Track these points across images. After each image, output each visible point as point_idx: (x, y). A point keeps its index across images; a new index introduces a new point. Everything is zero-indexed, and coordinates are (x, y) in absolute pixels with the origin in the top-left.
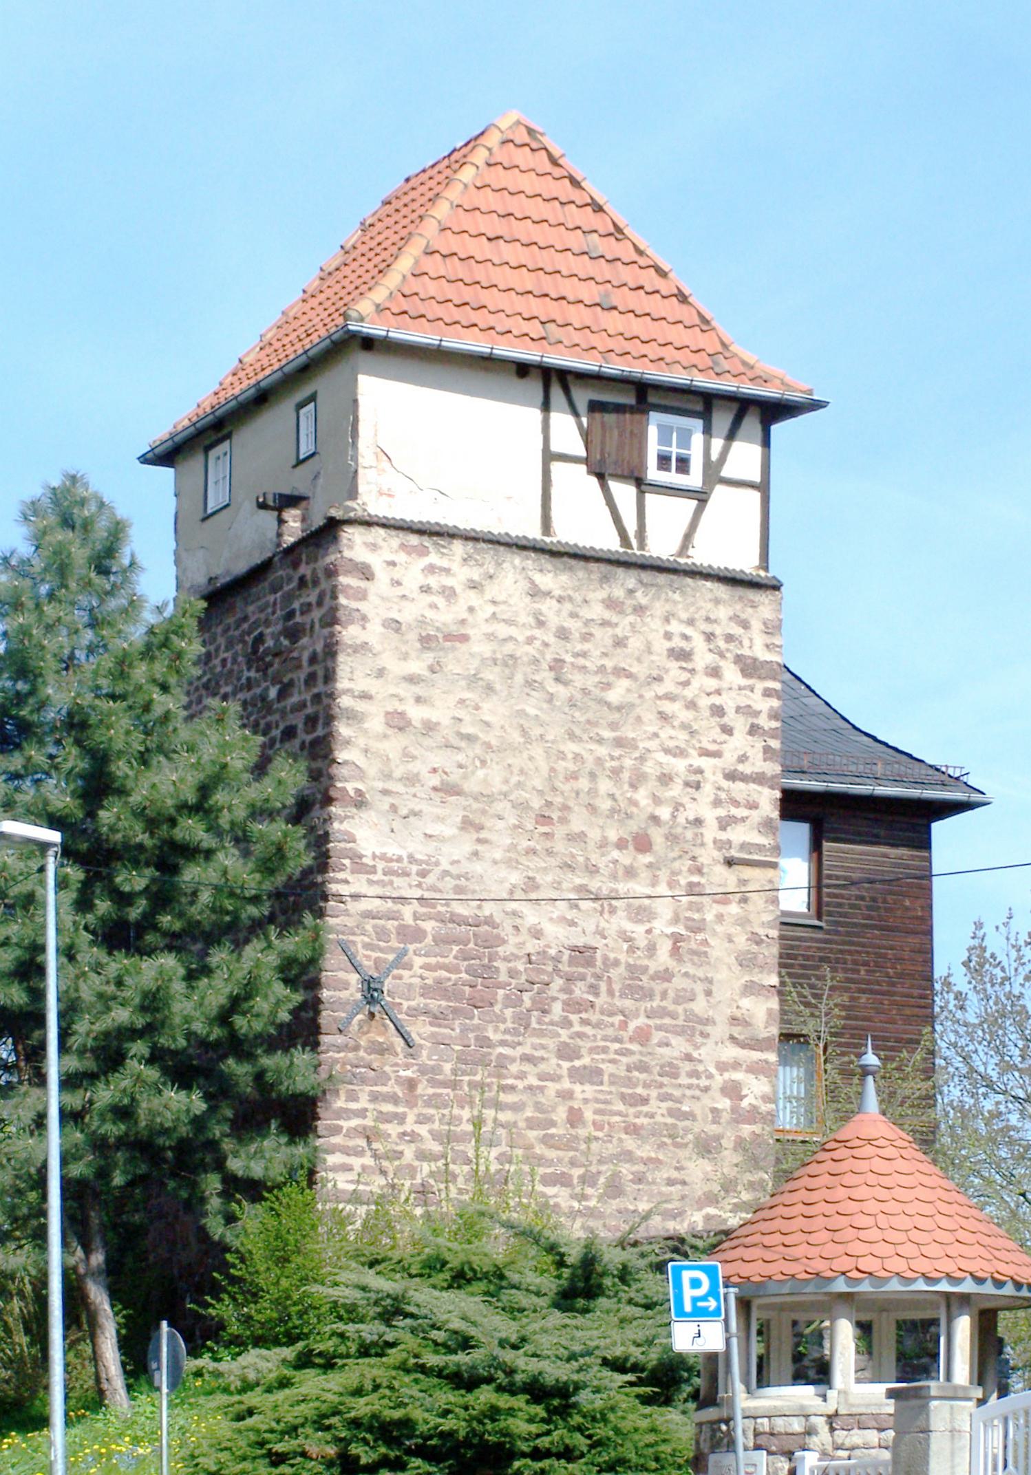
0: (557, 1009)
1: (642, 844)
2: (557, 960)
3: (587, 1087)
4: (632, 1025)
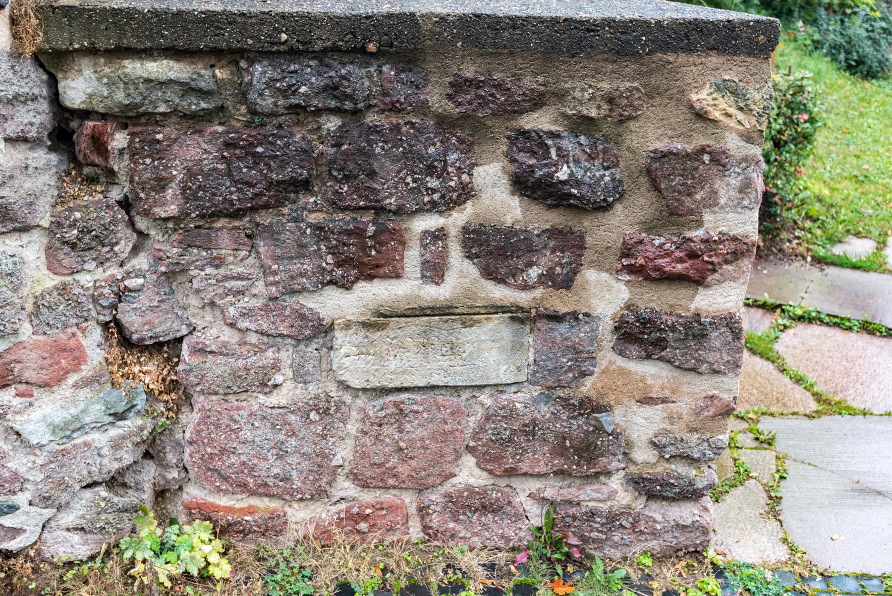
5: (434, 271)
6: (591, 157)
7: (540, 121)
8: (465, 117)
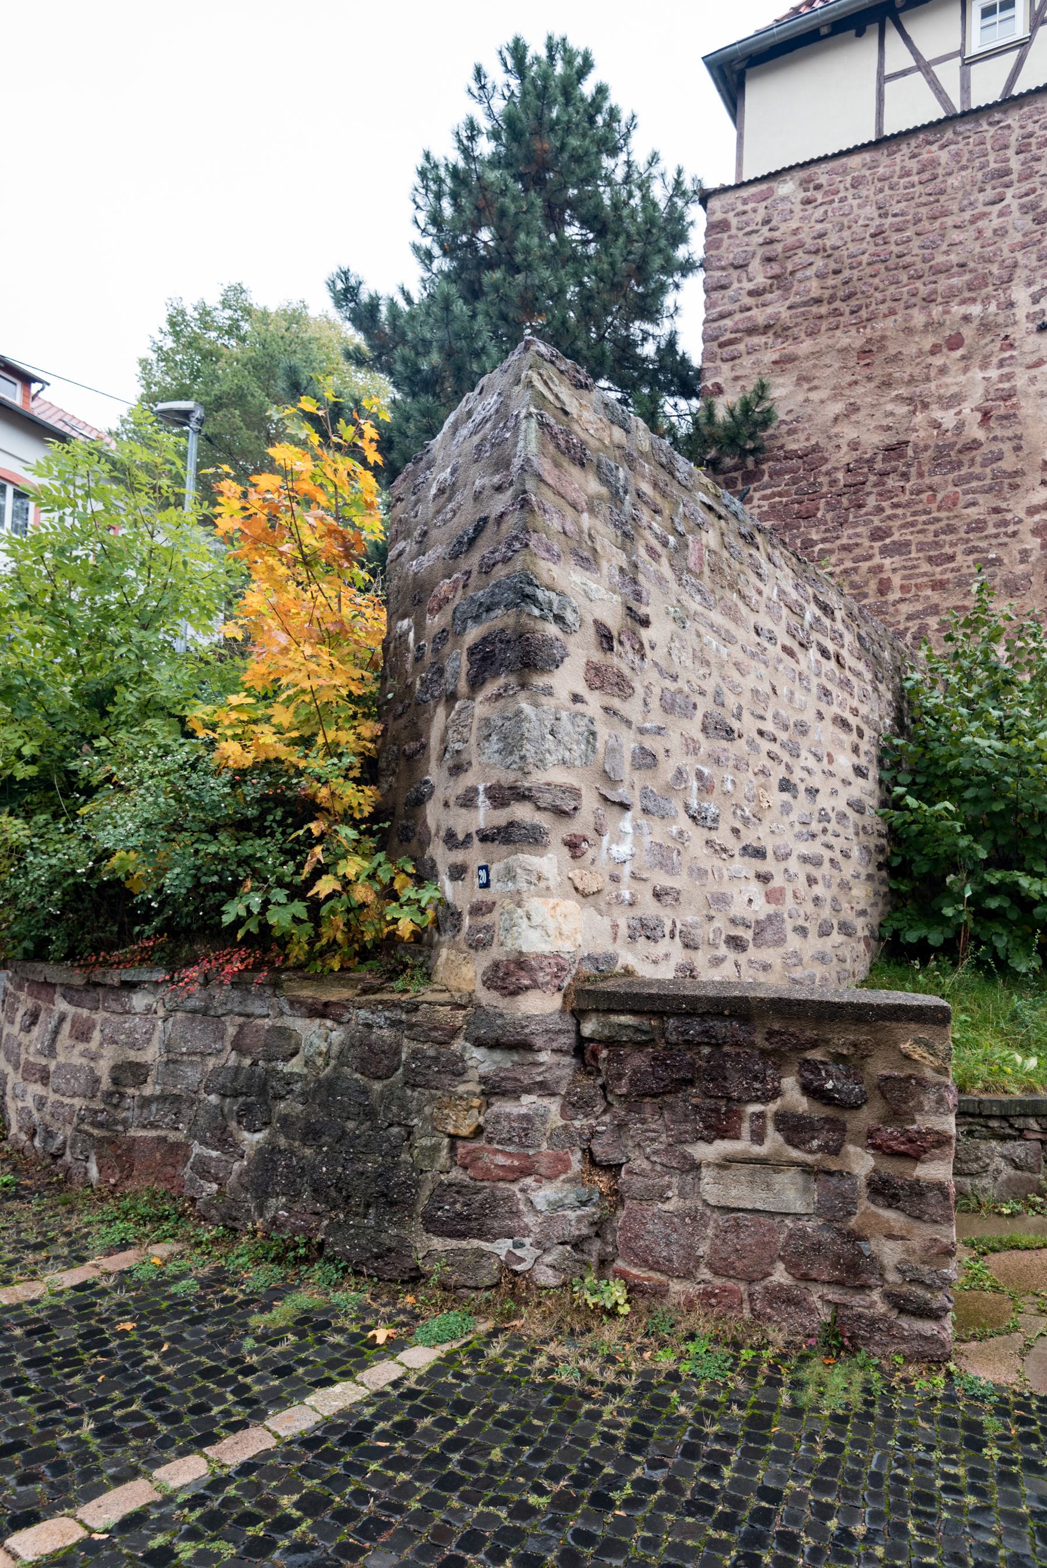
0: (872, 501)
1: (955, 342)
2: (871, 461)
3: (896, 558)
5: (758, 1137)
6: (847, 1077)
7: (816, 1055)
8: (775, 1050)
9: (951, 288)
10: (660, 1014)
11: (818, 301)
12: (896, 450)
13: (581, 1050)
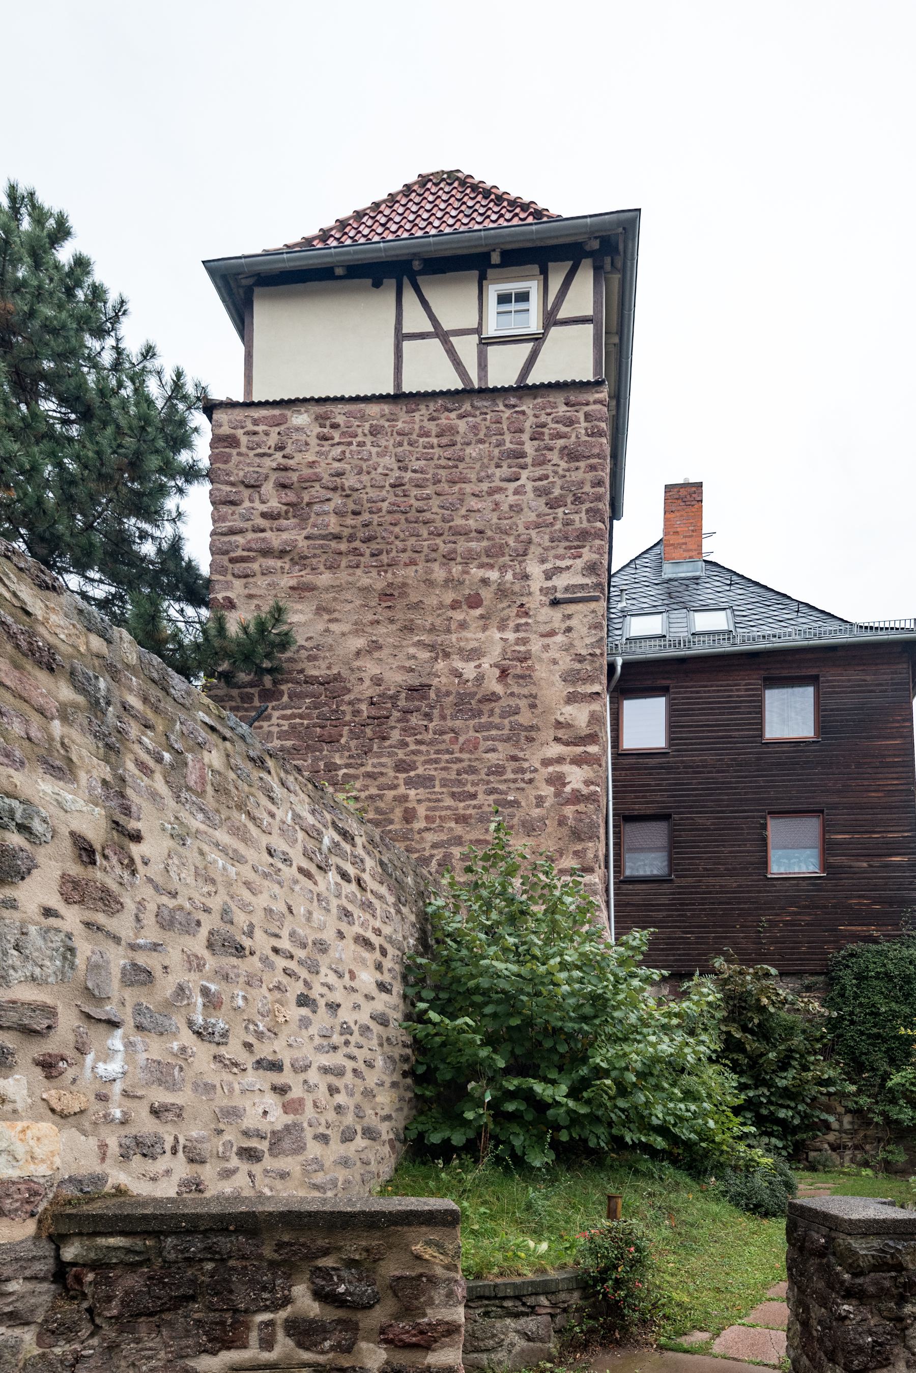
0: (396, 735)
1: (474, 602)
2: (394, 698)
3: (421, 790)
4: (461, 739)
5: (267, 1344)
6: (359, 1280)
7: (327, 1262)
8: (285, 1261)
9: (470, 550)
10: (156, 1234)
11: (337, 537)
12: (418, 691)
13: (61, 1274)
